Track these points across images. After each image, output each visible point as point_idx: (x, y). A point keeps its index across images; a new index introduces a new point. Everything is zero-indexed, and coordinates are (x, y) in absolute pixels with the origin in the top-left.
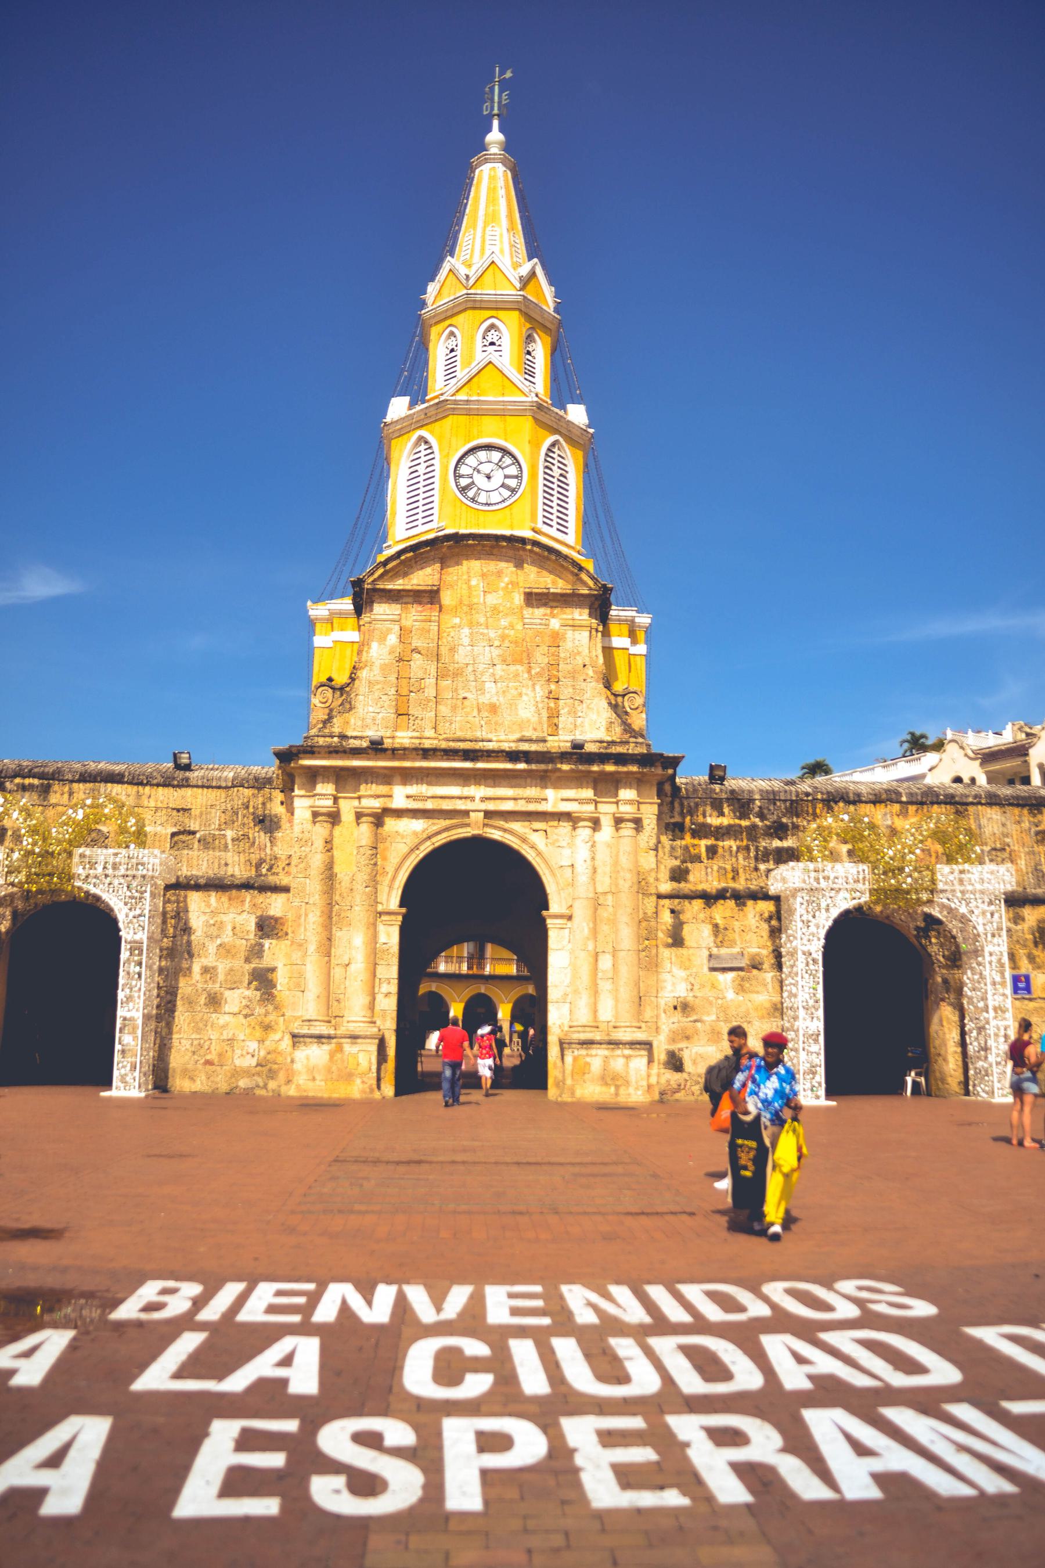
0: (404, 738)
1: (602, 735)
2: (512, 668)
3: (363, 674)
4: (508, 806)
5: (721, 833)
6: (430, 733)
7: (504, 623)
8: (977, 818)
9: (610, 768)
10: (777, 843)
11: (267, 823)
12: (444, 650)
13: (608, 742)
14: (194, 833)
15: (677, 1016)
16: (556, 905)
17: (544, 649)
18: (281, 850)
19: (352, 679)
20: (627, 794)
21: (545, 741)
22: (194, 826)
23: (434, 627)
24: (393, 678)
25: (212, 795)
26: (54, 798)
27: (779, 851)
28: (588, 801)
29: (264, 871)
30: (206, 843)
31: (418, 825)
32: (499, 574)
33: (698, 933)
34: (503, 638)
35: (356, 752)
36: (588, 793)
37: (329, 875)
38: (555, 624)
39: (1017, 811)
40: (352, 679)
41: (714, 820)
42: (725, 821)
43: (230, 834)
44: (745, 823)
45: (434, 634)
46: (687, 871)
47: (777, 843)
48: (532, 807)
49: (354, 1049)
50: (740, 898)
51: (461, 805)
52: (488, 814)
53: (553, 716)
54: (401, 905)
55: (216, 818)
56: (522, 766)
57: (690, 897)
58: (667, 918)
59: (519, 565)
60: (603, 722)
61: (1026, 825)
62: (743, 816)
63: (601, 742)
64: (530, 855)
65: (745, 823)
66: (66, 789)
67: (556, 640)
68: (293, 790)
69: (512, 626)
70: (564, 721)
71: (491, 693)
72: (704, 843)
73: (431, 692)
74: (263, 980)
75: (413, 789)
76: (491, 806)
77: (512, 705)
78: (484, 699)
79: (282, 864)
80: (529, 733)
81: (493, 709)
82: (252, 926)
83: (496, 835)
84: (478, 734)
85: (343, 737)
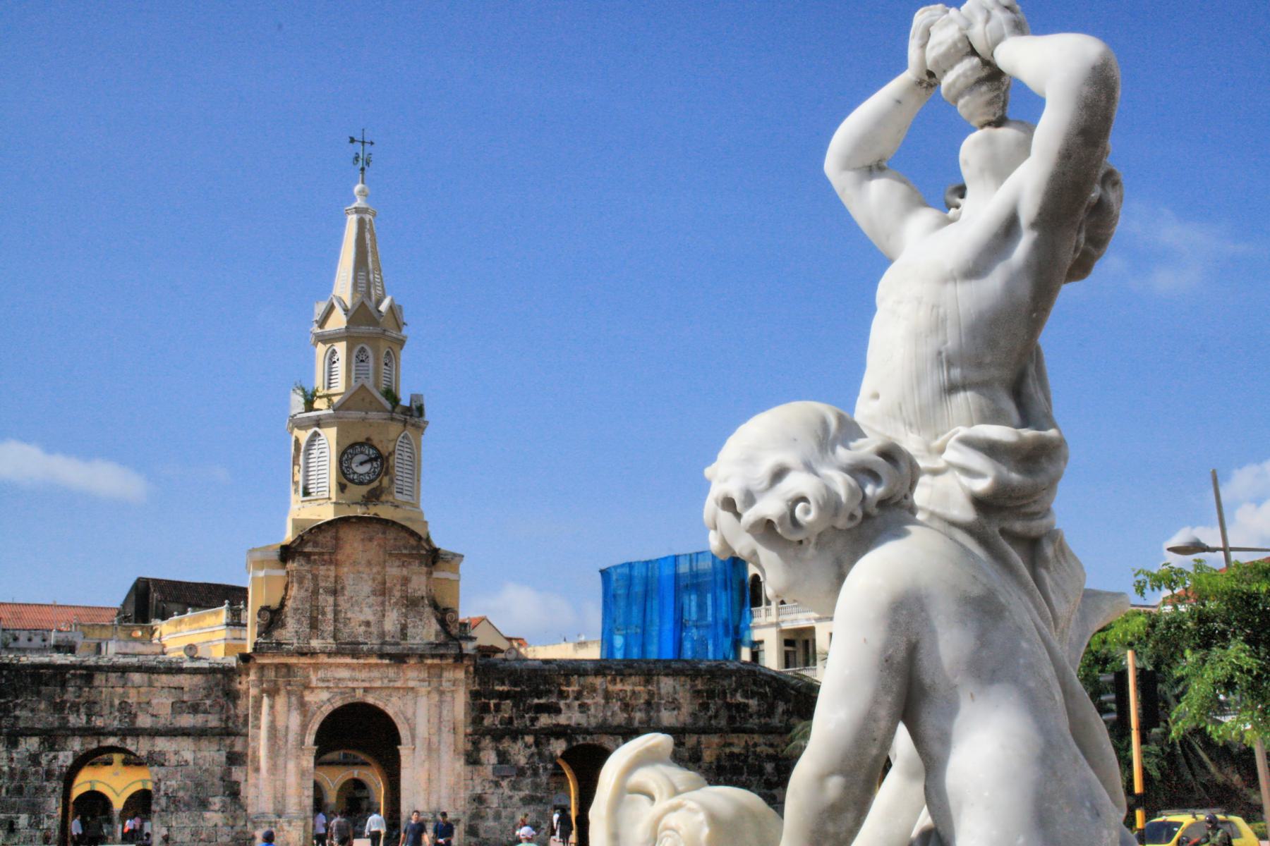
0: (315, 643)
1: (433, 639)
2: (380, 599)
3: (290, 604)
4: (378, 684)
5: (503, 696)
6: (331, 641)
7: (375, 570)
8: (658, 683)
9: (436, 661)
10: (536, 701)
11: (232, 696)
12: (339, 587)
13: (438, 645)
14: (184, 702)
15: (476, 804)
16: (403, 740)
17: (398, 587)
18: (240, 711)
19: (282, 605)
20: (448, 675)
21: (397, 644)
22: (185, 698)
23: (332, 574)
24: (307, 606)
25: (198, 680)
26: (96, 683)
27: (538, 705)
28: (423, 680)
29: (230, 724)
30: (195, 709)
31: (325, 695)
32: (371, 540)
33: (489, 757)
34: (374, 580)
35: (290, 654)
36: (424, 675)
37: (273, 728)
38: (405, 572)
39: (683, 679)
40: (282, 605)
41: (500, 688)
42: (505, 688)
43: (208, 702)
44: (518, 689)
45: (332, 579)
46: (483, 719)
47: (536, 701)
48: (391, 684)
49: (291, 829)
50: (515, 735)
51: (351, 684)
52: (366, 690)
53: (404, 628)
54: (316, 743)
55: (202, 693)
56: (387, 661)
57: (483, 735)
58: (469, 747)
59: (384, 533)
60: (433, 632)
61: (688, 687)
62: (515, 686)
63: (431, 644)
64: (390, 711)
65: (518, 689)
66: (103, 677)
67: (406, 581)
68: (248, 675)
69: (378, 573)
70: (410, 631)
71: (368, 614)
72: (492, 702)
73: (330, 616)
74: (233, 792)
75: (321, 674)
76: (367, 685)
77: (381, 622)
78: (362, 618)
79: (241, 720)
80: (387, 639)
81: (368, 624)
82: (224, 759)
83: (370, 700)
84: (361, 639)
85: (279, 644)
